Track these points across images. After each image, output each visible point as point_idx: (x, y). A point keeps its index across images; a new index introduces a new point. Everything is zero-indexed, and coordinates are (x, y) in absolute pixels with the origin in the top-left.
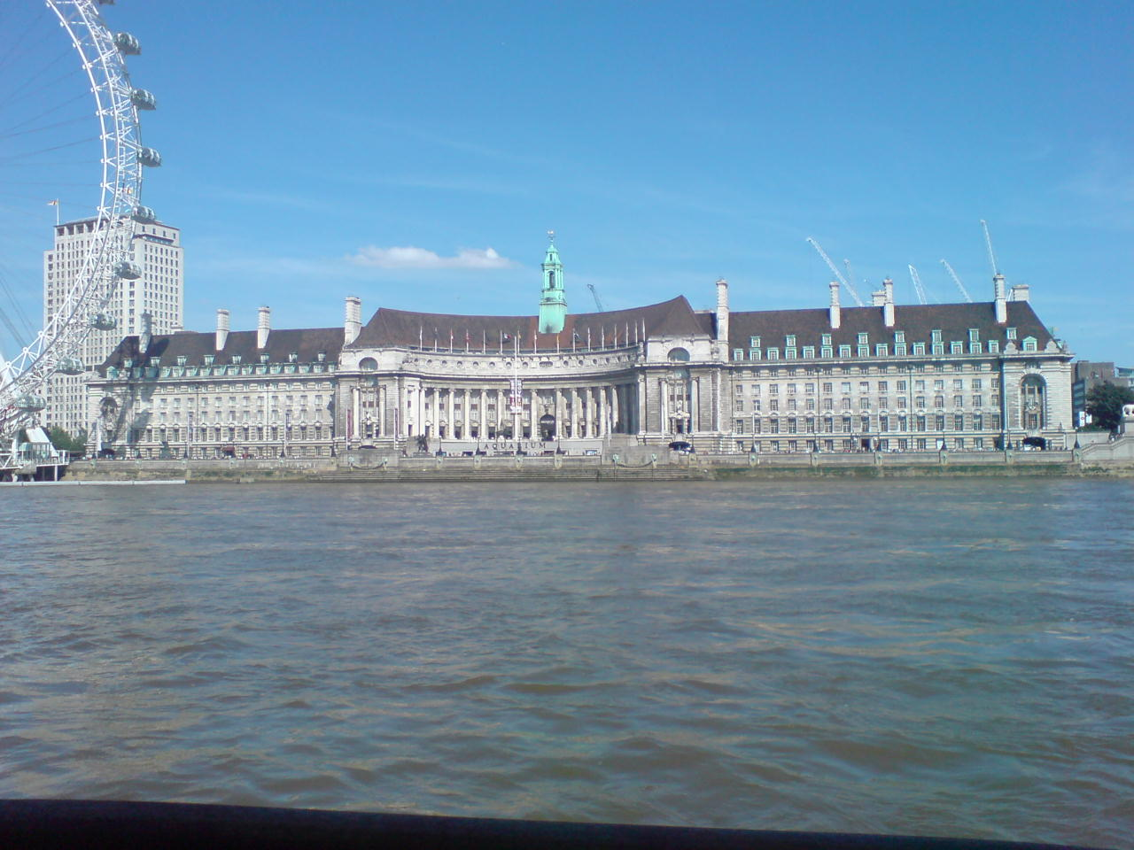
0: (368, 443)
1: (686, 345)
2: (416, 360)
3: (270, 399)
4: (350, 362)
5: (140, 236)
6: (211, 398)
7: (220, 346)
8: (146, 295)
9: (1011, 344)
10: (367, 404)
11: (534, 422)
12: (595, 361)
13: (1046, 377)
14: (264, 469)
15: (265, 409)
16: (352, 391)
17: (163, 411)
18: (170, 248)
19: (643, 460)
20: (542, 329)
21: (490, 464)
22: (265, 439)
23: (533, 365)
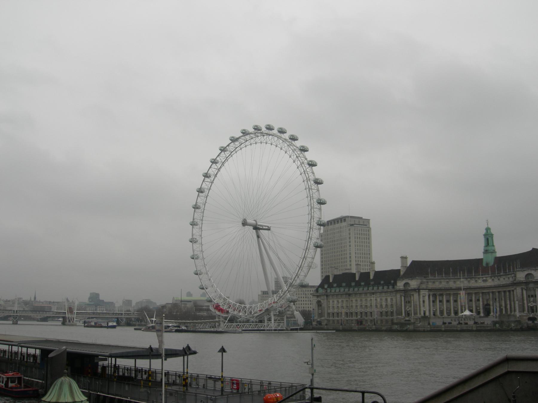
0: (407, 319)
1: (532, 272)
2: (427, 282)
3: (374, 300)
4: (400, 285)
5: (352, 225)
6: (354, 300)
7: (357, 279)
10: (408, 302)
11: (481, 307)
12: (504, 279)
15: (373, 304)
22: (373, 317)
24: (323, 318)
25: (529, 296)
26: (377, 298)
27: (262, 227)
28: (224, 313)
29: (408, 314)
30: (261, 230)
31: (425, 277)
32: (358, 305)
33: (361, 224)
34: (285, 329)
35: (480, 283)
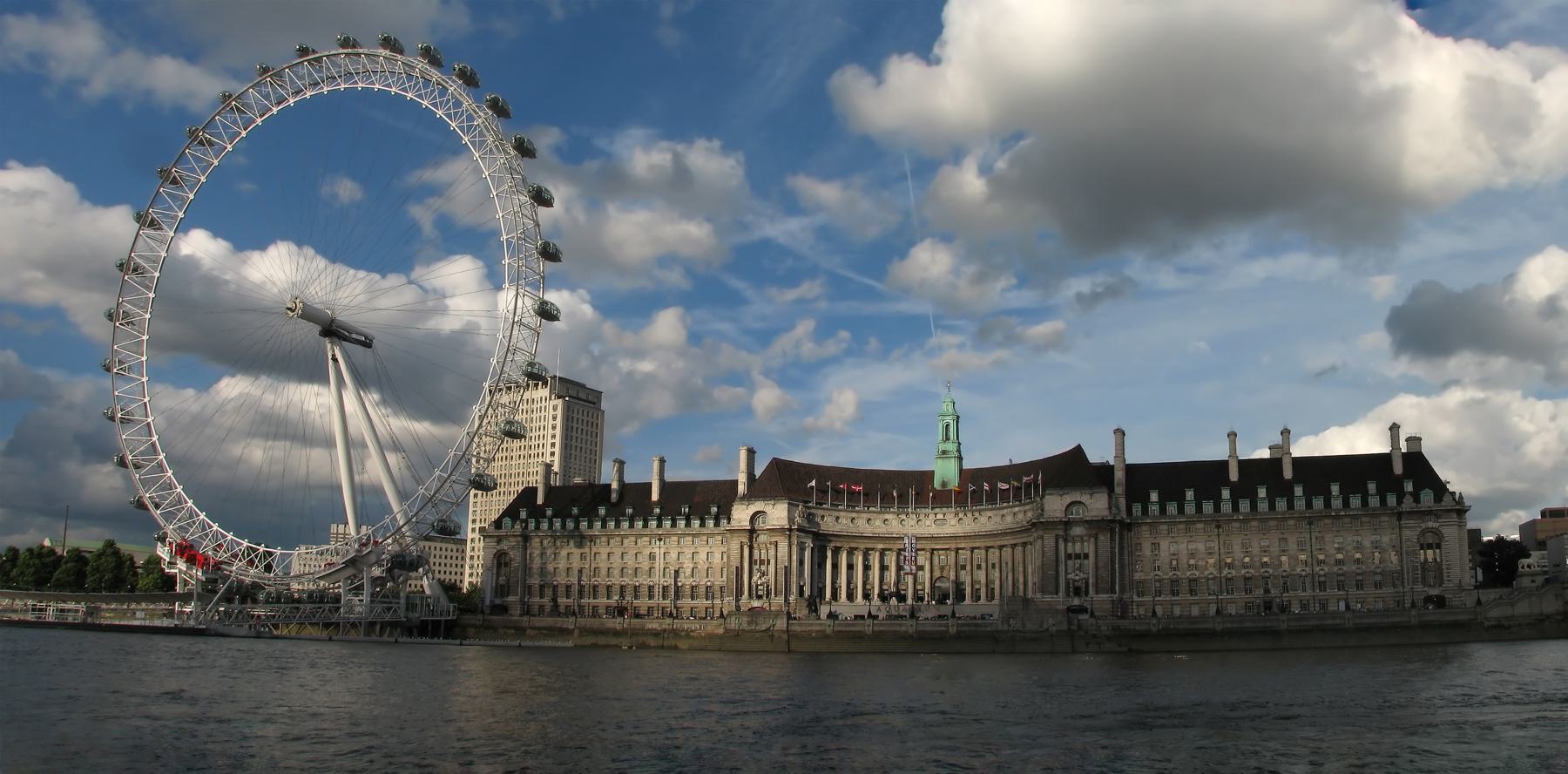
4: (741, 514)
9: (1408, 496)
13: (1445, 530)
14: (652, 629)
19: (1041, 627)
21: (882, 628)
23: (928, 523)
25: (1069, 557)
34: (405, 620)
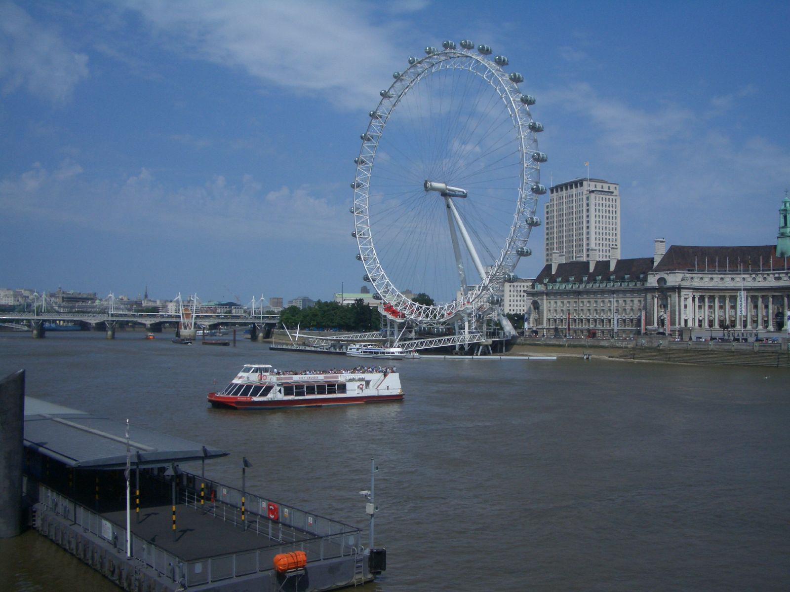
0: (661, 330)
2: (692, 278)
4: (652, 281)
5: (593, 191)
7: (591, 270)
8: (596, 228)
11: (771, 317)
15: (612, 308)
16: (653, 298)
17: (562, 309)
18: (611, 197)
20: (778, 254)
23: (770, 279)
24: (540, 327)
26: (619, 299)
27: (454, 193)
28: (398, 317)
29: (662, 322)
30: (452, 198)
31: (689, 271)
32: (590, 308)
33: (604, 190)
35: (771, 282)
